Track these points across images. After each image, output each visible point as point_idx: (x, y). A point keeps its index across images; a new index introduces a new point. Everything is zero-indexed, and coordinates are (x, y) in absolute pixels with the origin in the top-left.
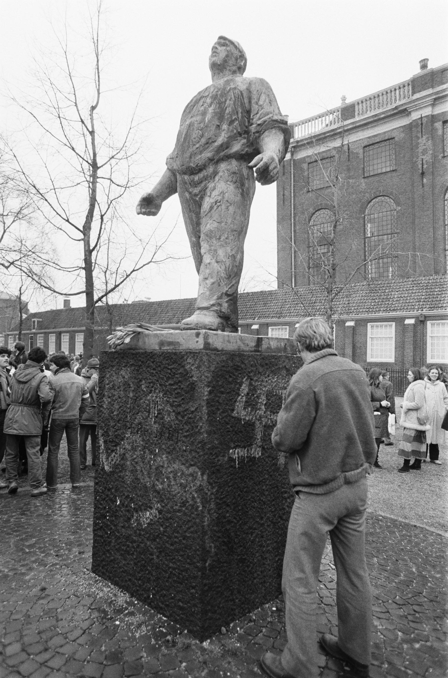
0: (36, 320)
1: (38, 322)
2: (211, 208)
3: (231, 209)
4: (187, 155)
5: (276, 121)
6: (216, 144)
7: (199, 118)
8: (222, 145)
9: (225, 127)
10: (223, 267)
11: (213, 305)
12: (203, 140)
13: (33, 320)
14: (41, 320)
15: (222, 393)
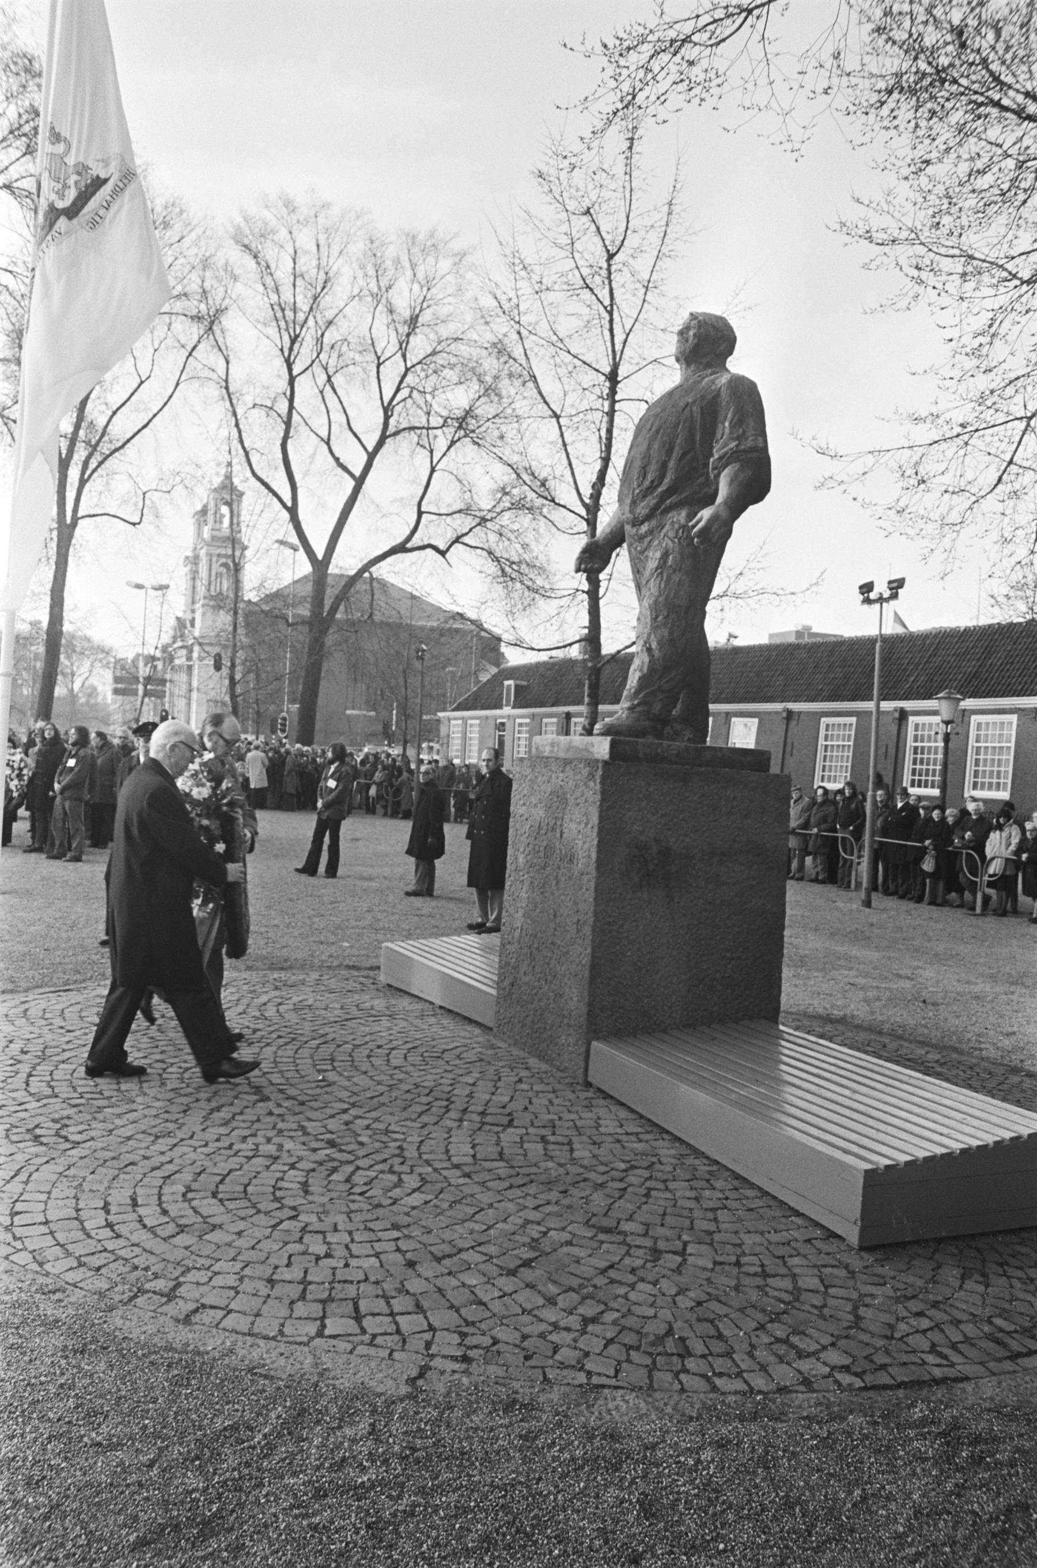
0: (511, 682)
1: (516, 686)
2: (652, 575)
3: (676, 578)
4: (628, 501)
5: (744, 451)
6: (660, 490)
7: (643, 448)
8: (667, 491)
9: (672, 464)
10: (657, 654)
11: (638, 705)
12: (647, 483)
13: (506, 683)
14: (524, 683)
15: (629, 809)
